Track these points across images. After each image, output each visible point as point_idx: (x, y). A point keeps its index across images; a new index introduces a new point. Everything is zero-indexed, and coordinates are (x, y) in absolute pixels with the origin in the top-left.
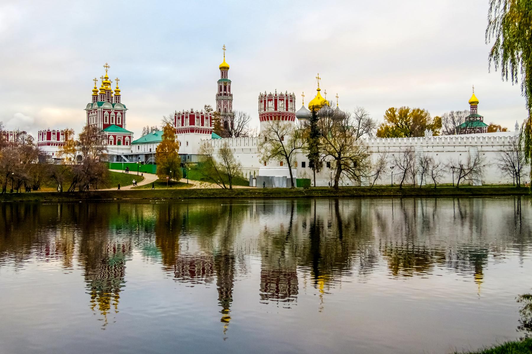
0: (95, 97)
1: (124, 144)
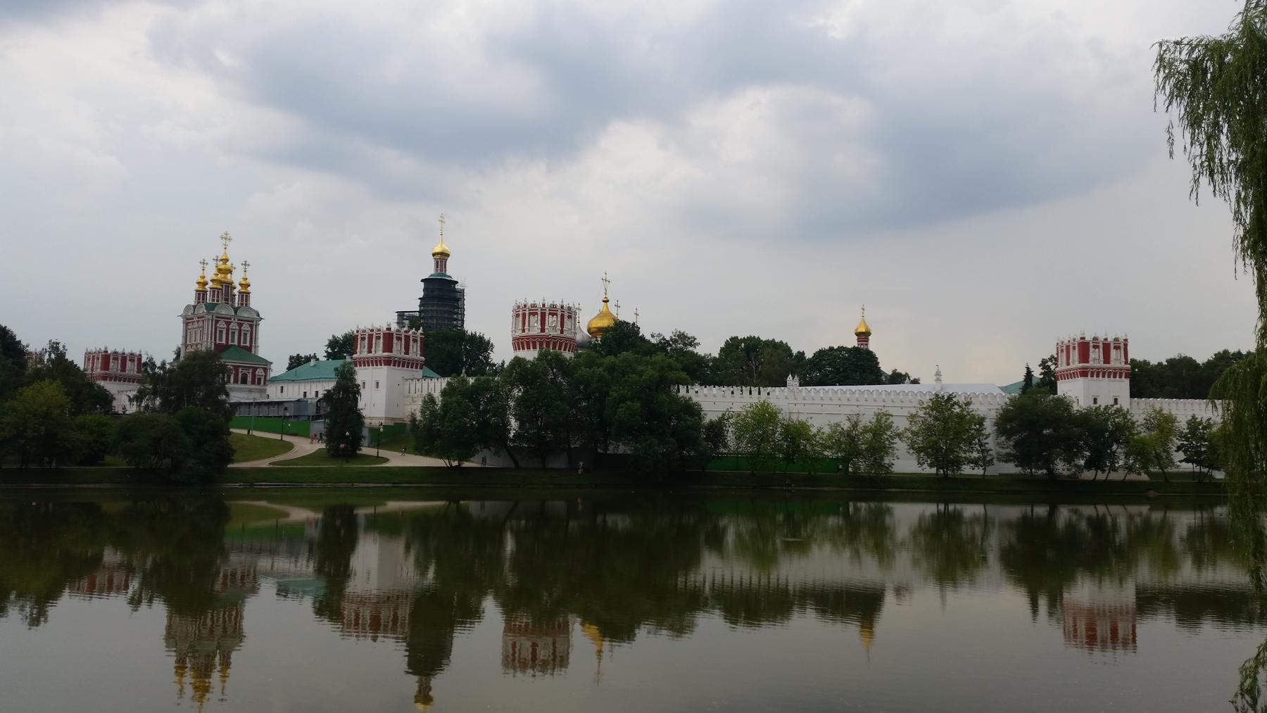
0: (201, 295)
1: (253, 383)
